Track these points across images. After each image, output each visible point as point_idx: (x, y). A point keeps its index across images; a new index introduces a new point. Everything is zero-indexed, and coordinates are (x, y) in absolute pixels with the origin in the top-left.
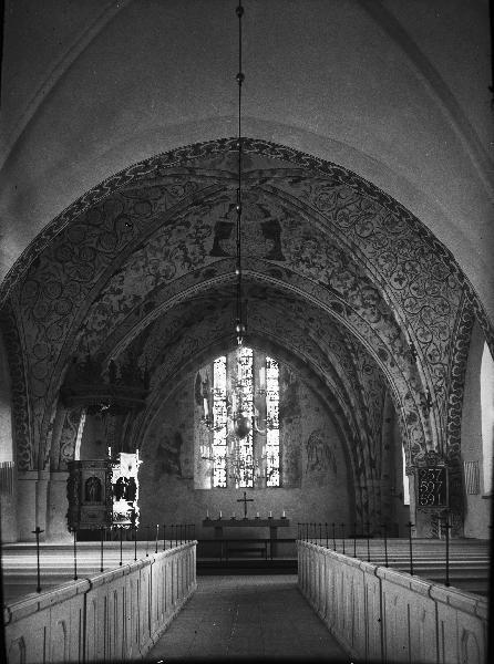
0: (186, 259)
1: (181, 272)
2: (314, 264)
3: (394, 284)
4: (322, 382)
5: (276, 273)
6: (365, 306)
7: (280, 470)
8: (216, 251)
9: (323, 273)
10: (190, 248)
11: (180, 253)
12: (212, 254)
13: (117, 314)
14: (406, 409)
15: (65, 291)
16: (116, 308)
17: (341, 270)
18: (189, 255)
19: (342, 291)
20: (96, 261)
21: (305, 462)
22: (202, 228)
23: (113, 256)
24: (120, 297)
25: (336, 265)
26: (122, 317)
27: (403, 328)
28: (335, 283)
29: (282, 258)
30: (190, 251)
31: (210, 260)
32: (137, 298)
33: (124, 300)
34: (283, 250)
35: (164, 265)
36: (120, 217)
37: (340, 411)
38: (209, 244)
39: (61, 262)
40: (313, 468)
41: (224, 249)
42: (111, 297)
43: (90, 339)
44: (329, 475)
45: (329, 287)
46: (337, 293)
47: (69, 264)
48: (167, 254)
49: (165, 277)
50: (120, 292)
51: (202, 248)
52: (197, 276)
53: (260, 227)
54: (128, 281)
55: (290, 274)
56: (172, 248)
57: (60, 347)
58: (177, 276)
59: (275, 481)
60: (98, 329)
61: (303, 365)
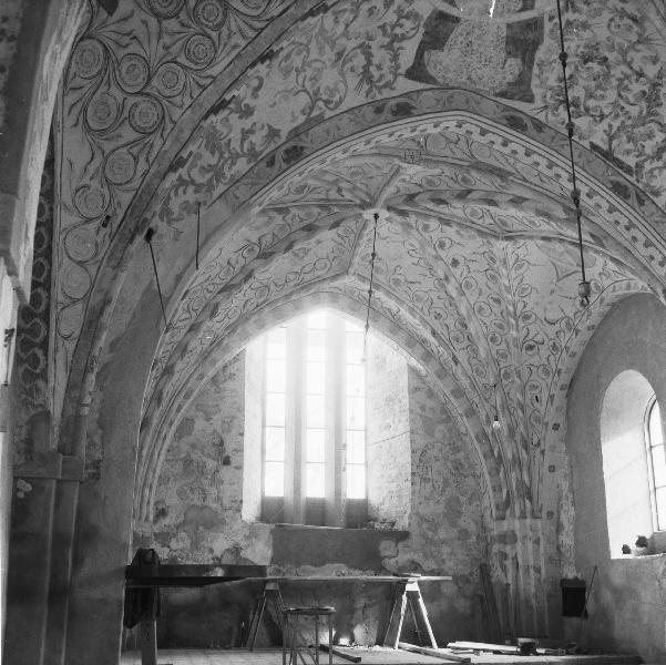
0: (366, 76)
1: (354, 99)
2: (587, 110)
5: (515, 123)
8: (417, 72)
9: (604, 125)
10: (380, 55)
11: (360, 61)
12: (410, 74)
13: (235, 157)
15: (154, 82)
16: (235, 145)
17: (642, 120)
18: (373, 69)
19: (631, 161)
20: (224, 28)
22: (407, 17)
23: (258, 25)
24: (247, 123)
25: (634, 111)
26: (242, 165)
28: (621, 148)
29: (531, 100)
30: (375, 61)
31: (405, 85)
32: (273, 133)
33: (252, 131)
34: (535, 82)
35: (329, 78)
38: (407, 59)
39: (157, 15)
41: (432, 72)
43: (183, 198)
45: (608, 155)
46: (620, 164)
47: (172, 25)
48: (339, 55)
49: (327, 102)
51: (395, 58)
52: (379, 111)
53: (504, 33)
54: (261, 104)
55: (540, 126)
57: (126, 198)
58: (344, 107)
60: (200, 180)
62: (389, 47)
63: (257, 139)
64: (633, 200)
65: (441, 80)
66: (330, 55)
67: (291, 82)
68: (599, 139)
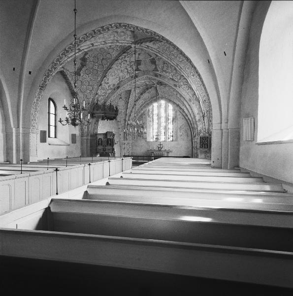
1: (127, 77)
3: (192, 77)
4: (184, 112)
5: (156, 76)
6: (184, 85)
7: (172, 136)
8: (137, 69)
10: (129, 69)
13: (108, 90)
14: (197, 118)
19: (176, 80)
21: (179, 134)
26: (110, 91)
27: (195, 92)
32: (114, 85)
35: (121, 74)
36: (103, 59)
37: (189, 119)
40: (181, 136)
42: (106, 85)
44: (186, 138)
45: (173, 79)
47: (90, 75)
50: (108, 83)
51: (133, 68)
55: (160, 75)
56: (123, 69)
57: (91, 100)
58: (126, 78)
59: (171, 139)
61: (178, 105)
62: (131, 67)
63: (111, 86)
64: (178, 88)
65: (142, 70)
66: (119, 71)
67: (114, 77)
68: (171, 77)
